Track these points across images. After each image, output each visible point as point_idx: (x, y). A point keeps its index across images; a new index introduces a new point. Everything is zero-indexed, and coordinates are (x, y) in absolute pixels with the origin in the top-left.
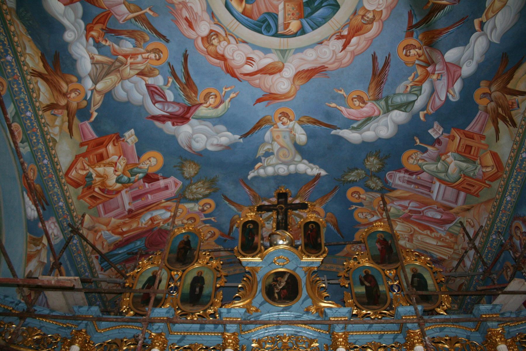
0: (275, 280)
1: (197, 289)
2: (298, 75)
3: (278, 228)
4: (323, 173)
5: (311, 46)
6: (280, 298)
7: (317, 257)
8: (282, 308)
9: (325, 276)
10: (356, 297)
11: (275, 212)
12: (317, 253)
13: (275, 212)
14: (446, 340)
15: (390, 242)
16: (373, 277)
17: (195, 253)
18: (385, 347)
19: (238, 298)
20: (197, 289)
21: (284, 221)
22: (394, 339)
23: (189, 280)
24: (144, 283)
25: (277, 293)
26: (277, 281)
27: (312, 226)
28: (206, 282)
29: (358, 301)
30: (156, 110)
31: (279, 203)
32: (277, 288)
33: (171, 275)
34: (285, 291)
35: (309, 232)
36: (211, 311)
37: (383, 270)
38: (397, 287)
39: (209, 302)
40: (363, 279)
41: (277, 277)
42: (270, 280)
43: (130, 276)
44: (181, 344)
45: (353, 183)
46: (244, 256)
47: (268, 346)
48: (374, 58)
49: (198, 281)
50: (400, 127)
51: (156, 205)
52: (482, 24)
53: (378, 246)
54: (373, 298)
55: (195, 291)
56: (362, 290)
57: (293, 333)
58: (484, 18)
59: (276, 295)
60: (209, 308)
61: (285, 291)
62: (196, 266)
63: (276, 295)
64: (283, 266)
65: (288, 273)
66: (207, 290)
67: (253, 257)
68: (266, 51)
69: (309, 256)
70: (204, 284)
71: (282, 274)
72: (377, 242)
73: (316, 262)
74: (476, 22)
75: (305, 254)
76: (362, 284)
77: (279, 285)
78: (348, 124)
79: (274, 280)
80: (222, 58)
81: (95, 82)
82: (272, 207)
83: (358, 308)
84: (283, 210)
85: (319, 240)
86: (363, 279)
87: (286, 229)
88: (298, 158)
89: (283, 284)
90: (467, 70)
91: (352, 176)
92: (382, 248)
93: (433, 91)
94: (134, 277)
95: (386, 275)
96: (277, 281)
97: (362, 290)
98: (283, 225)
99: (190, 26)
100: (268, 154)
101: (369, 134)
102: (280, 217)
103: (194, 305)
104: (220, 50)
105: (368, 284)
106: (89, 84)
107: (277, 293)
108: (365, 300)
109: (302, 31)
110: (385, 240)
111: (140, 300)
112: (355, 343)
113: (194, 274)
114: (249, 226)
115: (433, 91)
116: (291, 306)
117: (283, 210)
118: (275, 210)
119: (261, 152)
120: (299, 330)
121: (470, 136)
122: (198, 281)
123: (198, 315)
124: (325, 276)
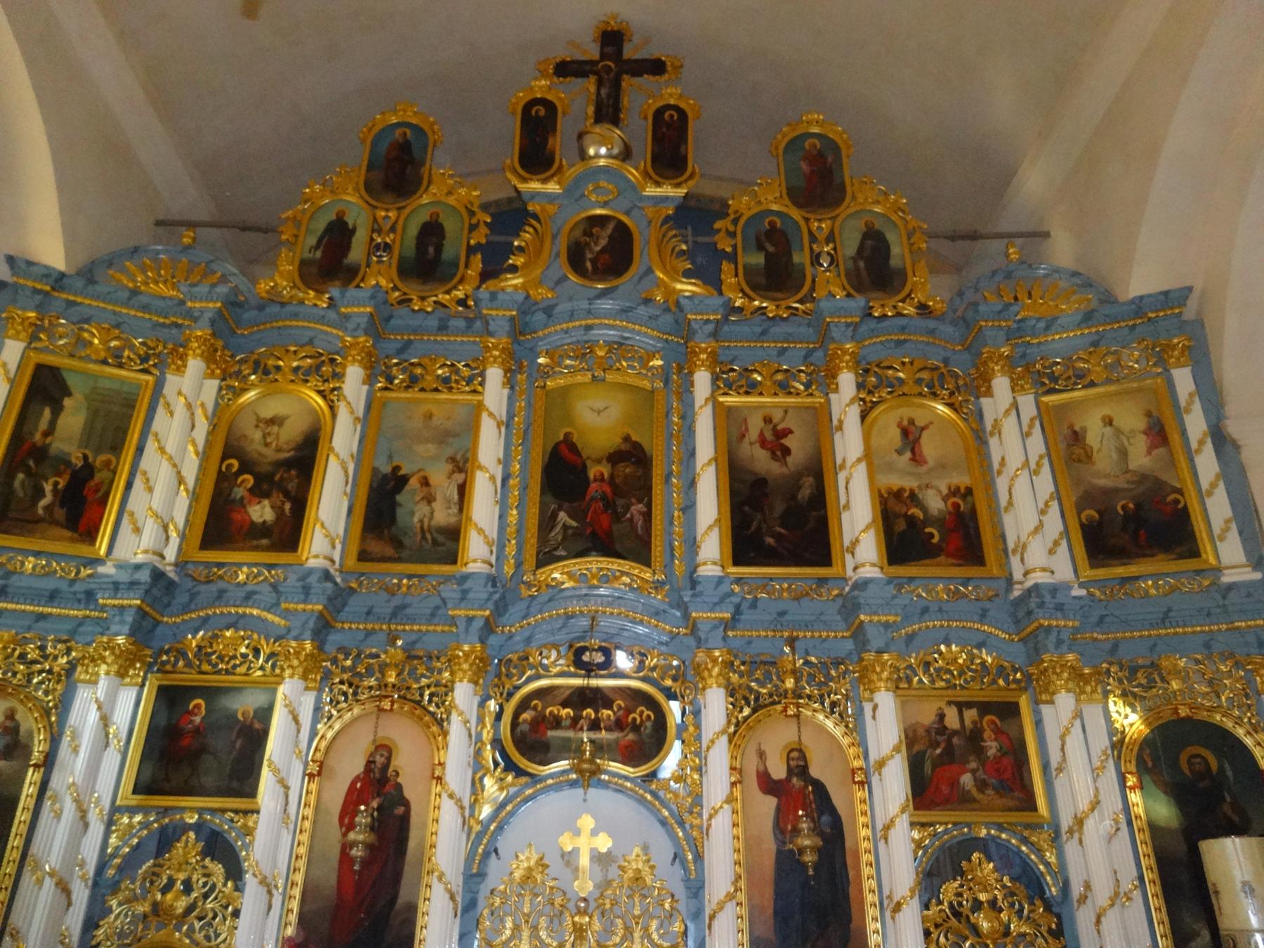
0: (587, 233)
1: (431, 250)
3: (599, 119)
6: (596, 269)
7: (678, 185)
8: (597, 292)
9: (689, 228)
10: (745, 274)
11: (593, 79)
12: (677, 177)
13: (593, 79)
14: (903, 363)
15: (830, 159)
16: (783, 233)
17: (425, 171)
18: (787, 371)
19: (514, 269)
20: (431, 250)
21: (611, 101)
22: (806, 357)
23: (413, 230)
24: (319, 233)
25: (591, 260)
26: (591, 235)
27: (672, 116)
28: (448, 235)
29: (748, 283)
31: (603, 56)
32: (591, 250)
33: (375, 220)
34: (607, 256)
35: (664, 129)
36: (460, 294)
37: (807, 220)
38: (829, 259)
39: (455, 275)
40: (763, 238)
41: (592, 226)
42: (578, 233)
43: (288, 218)
44: (405, 356)
46: (525, 180)
47: (568, 362)
49: (432, 232)
53: (804, 166)
54: (778, 275)
55: (426, 253)
56: (758, 259)
57: (616, 339)
59: (589, 265)
60: (455, 288)
61: (607, 256)
62: (425, 200)
63: (589, 265)
64: (605, 205)
65: (614, 218)
66: (453, 247)
67: (545, 181)
69: (658, 184)
70: (443, 237)
71: (601, 221)
72: (804, 158)
73: (672, 198)
75: (651, 178)
76: (760, 247)
77: (596, 244)
79: (585, 233)
82: (587, 68)
83: (745, 295)
84: (612, 75)
85: (683, 148)
86: (763, 238)
87: (615, 121)
89: (603, 242)
92: (812, 172)
94: (296, 222)
95: (810, 232)
96: (591, 235)
97: (758, 259)
98: (608, 112)
102: (604, 92)
103: (425, 282)
105: (771, 249)
107: (591, 260)
108: (763, 281)
110: (821, 155)
111: (314, 270)
112: (732, 362)
113: (424, 217)
114: (537, 112)
116: (616, 288)
117: (612, 75)
118: (596, 73)
120: (627, 335)
122: (432, 232)
123: (435, 302)
124: (689, 228)
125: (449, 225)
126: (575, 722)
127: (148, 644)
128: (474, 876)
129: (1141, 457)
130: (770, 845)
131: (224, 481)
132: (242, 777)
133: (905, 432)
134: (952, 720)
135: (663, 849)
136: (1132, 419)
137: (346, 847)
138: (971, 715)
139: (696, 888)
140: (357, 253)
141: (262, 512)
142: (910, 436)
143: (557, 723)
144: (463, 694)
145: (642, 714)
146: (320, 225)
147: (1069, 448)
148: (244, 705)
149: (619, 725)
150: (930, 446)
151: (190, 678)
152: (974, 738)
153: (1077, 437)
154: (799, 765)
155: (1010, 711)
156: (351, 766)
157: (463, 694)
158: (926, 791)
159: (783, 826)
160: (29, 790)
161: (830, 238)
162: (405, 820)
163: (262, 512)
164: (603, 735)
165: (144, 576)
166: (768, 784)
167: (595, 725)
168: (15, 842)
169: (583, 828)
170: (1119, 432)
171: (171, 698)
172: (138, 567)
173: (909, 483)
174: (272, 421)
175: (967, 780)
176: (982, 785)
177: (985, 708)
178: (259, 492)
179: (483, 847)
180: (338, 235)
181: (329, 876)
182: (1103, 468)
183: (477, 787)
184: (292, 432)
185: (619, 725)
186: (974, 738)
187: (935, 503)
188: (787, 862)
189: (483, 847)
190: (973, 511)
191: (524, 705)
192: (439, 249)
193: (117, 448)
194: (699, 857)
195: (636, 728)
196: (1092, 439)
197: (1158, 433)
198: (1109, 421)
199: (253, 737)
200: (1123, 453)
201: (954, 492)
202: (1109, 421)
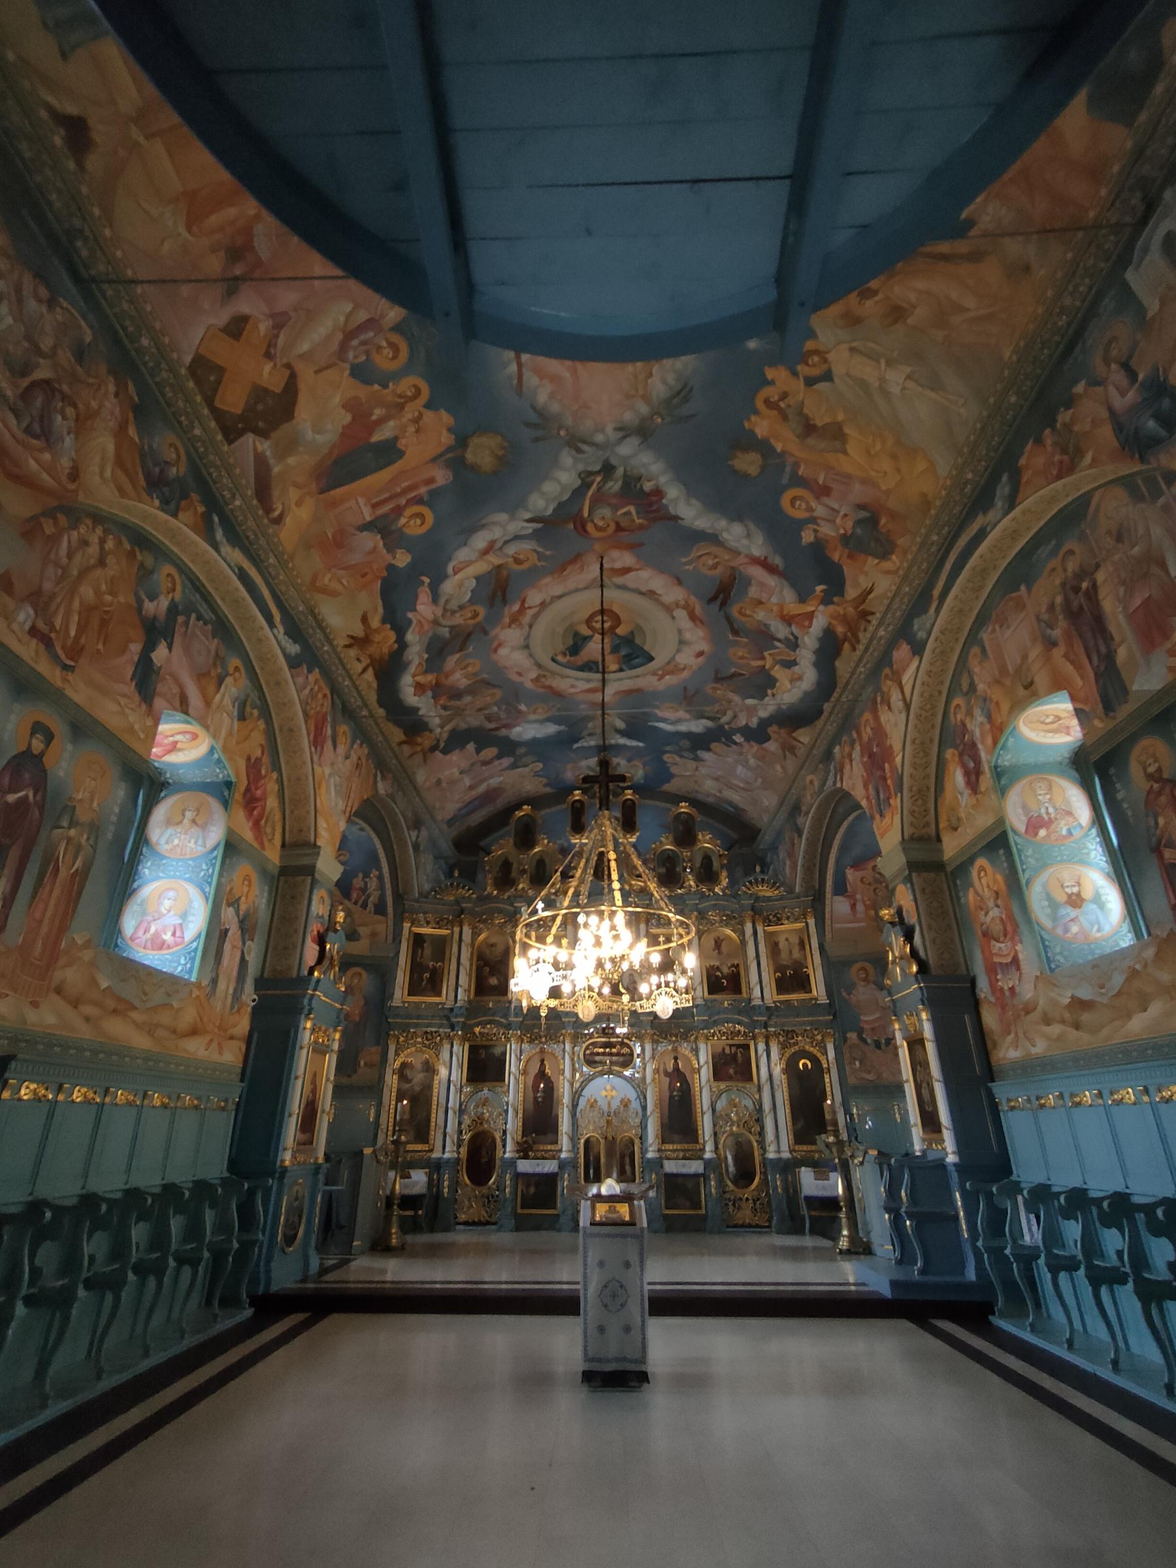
2: (617, 693)
4: (641, 744)
5: (630, 678)
23: (534, 863)
30: (492, 726)
45: (667, 752)
48: (685, 689)
50: (709, 730)
51: (492, 777)
52: (773, 695)
58: (774, 691)
68: (588, 681)
74: (769, 692)
76: (664, 865)
78: (664, 720)
80: (550, 687)
81: (442, 727)
88: (618, 736)
90: (763, 714)
91: (668, 748)
93: (735, 717)
99: (520, 674)
100: (590, 735)
101: (683, 728)
104: (547, 683)
106: (439, 730)
109: (621, 670)
115: (735, 717)
119: (585, 733)
121: (764, 749)
125: (547, 861)
126: (604, 1054)
127: (468, 1035)
128: (574, 1105)
129: (796, 954)
130: (667, 1094)
131: (478, 968)
132: (499, 1076)
133: (716, 942)
134: (727, 1051)
135: (631, 1094)
136: (795, 940)
137: (535, 1098)
138: (733, 1049)
139: (644, 1108)
140: (514, 874)
141: (493, 981)
142: (718, 943)
143: (598, 1054)
144: (568, 1047)
145: (625, 1050)
146: (500, 863)
147: (774, 949)
148: (497, 1051)
149: (618, 1054)
150: (724, 948)
151: (479, 1042)
152: (735, 1056)
153: (776, 944)
154: (676, 1068)
155: (746, 1047)
156: (534, 1069)
157: (568, 1047)
158: (718, 1075)
159: (671, 1088)
160: (436, 1082)
161: (690, 861)
162: (552, 1088)
163: (493, 981)
164: (614, 1058)
165: (463, 1010)
166: (667, 1074)
167: (611, 1054)
168: (435, 1099)
169: (607, 1089)
170: (790, 944)
171: (473, 1050)
172: (461, 1008)
173: (717, 964)
174: (492, 945)
175: (731, 1071)
176: (736, 1073)
177: (738, 1046)
178: (492, 974)
179: (576, 1096)
180: (506, 866)
181: (530, 1105)
182: (784, 958)
183: (573, 1076)
184: (500, 948)
185: (618, 1054)
186: (735, 1056)
187: (726, 970)
188: (671, 1097)
189: (576, 1096)
190: (739, 974)
191: (587, 1048)
192: (544, 871)
193: (443, 961)
194: (645, 1098)
195: (623, 1055)
196: (781, 946)
197: (802, 944)
198: (787, 939)
199: (501, 1062)
200: (791, 952)
201: (733, 966)
202: (787, 939)
